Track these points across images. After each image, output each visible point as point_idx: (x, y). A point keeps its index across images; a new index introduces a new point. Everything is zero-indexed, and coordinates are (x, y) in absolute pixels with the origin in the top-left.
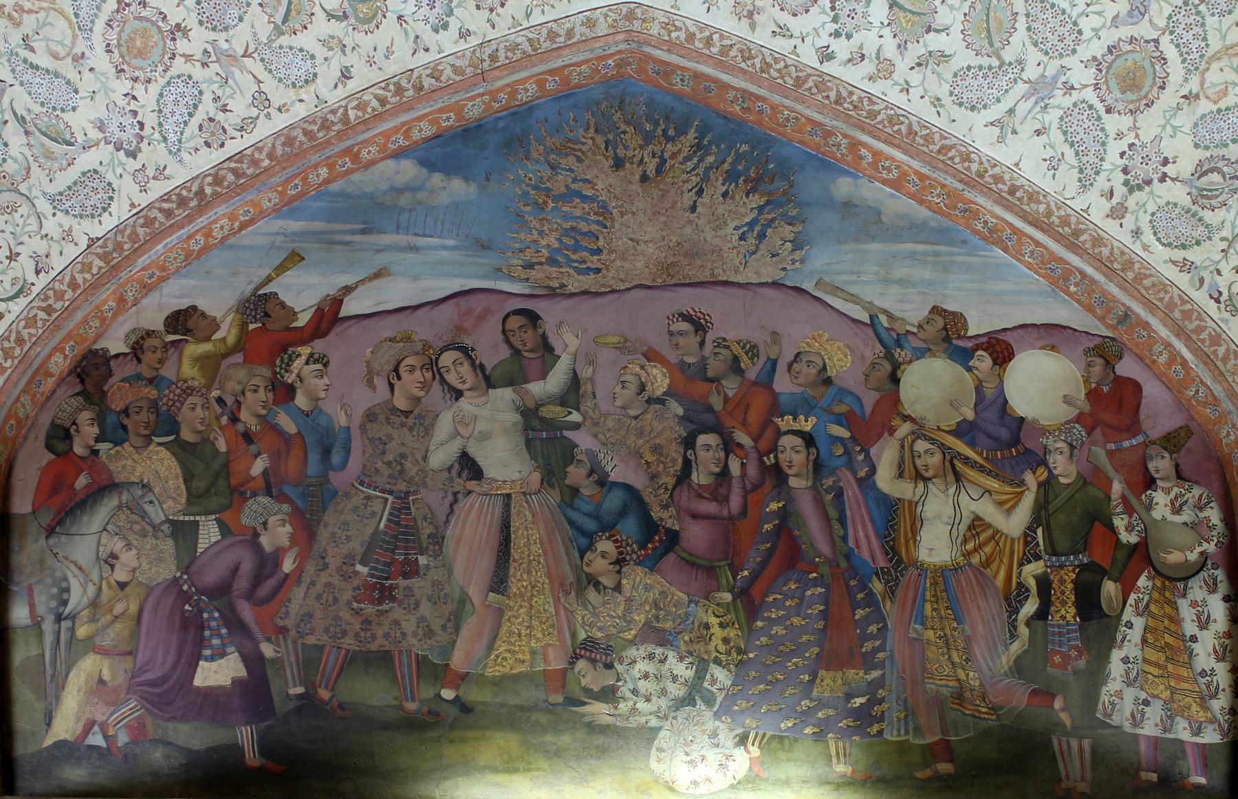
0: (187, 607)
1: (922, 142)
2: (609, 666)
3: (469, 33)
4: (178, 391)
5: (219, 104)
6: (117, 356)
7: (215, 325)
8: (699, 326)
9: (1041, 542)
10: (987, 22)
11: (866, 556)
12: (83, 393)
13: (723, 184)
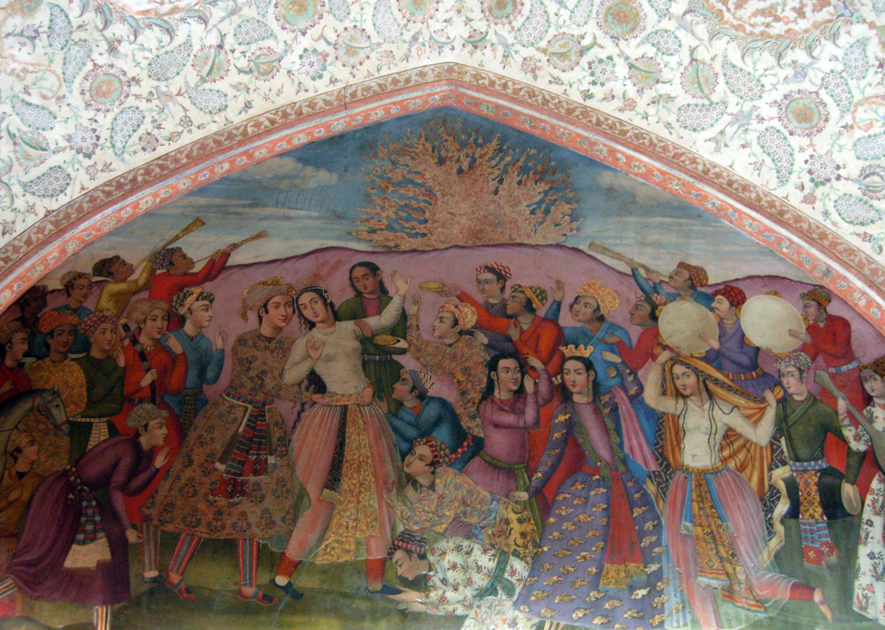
1: (660, 150)
2: (423, 557)
3: (337, 80)
4: (95, 319)
5: (156, 124)
6: (53, 291)
7: (131, 269)
8: (501, 276)
9: (785, 450)
11: (640, 461)
12: (22, 320)
13: (518, 176)
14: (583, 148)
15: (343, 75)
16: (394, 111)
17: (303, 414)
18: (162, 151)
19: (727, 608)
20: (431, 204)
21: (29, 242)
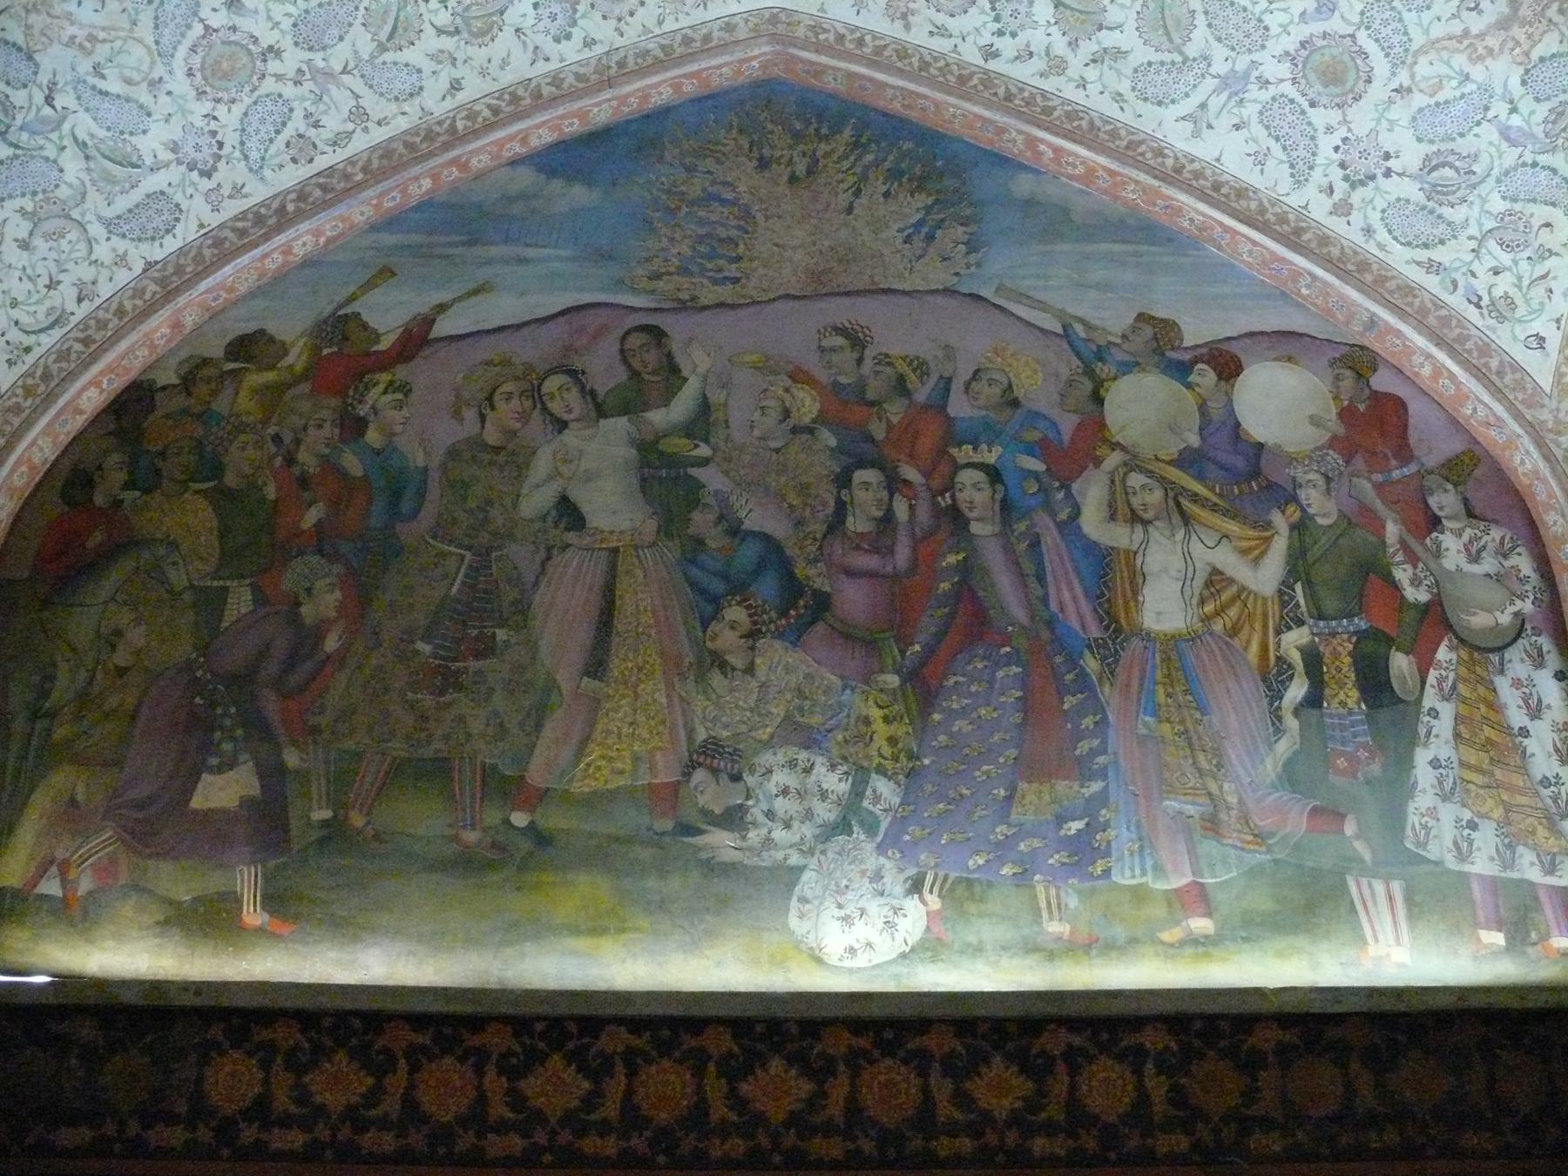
0: (198, 700)
2: (736, 778)
3: (594, 42)
6: (164, 388)
8: (857, 340)
9: (1302, 602)
10: (1163, 19)
14: (985, 139)
15: (604, 32)
16: (689, 88)
18: (322, 162)
19: (1208, 847)
20: (747, 232)
21: (120, 312)
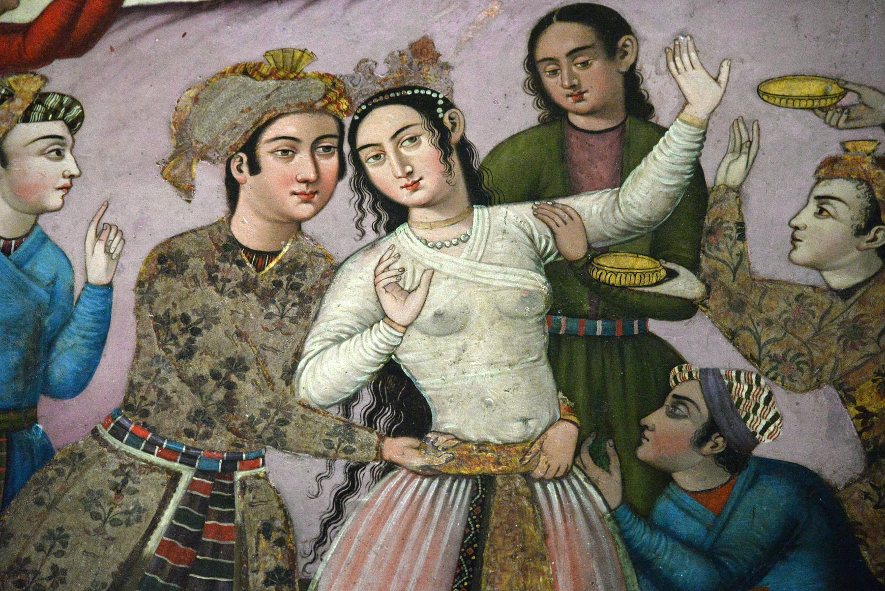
17: (351, 500)
